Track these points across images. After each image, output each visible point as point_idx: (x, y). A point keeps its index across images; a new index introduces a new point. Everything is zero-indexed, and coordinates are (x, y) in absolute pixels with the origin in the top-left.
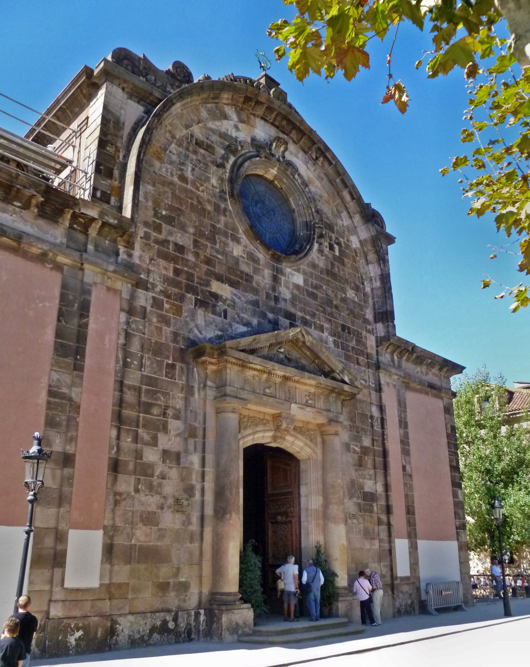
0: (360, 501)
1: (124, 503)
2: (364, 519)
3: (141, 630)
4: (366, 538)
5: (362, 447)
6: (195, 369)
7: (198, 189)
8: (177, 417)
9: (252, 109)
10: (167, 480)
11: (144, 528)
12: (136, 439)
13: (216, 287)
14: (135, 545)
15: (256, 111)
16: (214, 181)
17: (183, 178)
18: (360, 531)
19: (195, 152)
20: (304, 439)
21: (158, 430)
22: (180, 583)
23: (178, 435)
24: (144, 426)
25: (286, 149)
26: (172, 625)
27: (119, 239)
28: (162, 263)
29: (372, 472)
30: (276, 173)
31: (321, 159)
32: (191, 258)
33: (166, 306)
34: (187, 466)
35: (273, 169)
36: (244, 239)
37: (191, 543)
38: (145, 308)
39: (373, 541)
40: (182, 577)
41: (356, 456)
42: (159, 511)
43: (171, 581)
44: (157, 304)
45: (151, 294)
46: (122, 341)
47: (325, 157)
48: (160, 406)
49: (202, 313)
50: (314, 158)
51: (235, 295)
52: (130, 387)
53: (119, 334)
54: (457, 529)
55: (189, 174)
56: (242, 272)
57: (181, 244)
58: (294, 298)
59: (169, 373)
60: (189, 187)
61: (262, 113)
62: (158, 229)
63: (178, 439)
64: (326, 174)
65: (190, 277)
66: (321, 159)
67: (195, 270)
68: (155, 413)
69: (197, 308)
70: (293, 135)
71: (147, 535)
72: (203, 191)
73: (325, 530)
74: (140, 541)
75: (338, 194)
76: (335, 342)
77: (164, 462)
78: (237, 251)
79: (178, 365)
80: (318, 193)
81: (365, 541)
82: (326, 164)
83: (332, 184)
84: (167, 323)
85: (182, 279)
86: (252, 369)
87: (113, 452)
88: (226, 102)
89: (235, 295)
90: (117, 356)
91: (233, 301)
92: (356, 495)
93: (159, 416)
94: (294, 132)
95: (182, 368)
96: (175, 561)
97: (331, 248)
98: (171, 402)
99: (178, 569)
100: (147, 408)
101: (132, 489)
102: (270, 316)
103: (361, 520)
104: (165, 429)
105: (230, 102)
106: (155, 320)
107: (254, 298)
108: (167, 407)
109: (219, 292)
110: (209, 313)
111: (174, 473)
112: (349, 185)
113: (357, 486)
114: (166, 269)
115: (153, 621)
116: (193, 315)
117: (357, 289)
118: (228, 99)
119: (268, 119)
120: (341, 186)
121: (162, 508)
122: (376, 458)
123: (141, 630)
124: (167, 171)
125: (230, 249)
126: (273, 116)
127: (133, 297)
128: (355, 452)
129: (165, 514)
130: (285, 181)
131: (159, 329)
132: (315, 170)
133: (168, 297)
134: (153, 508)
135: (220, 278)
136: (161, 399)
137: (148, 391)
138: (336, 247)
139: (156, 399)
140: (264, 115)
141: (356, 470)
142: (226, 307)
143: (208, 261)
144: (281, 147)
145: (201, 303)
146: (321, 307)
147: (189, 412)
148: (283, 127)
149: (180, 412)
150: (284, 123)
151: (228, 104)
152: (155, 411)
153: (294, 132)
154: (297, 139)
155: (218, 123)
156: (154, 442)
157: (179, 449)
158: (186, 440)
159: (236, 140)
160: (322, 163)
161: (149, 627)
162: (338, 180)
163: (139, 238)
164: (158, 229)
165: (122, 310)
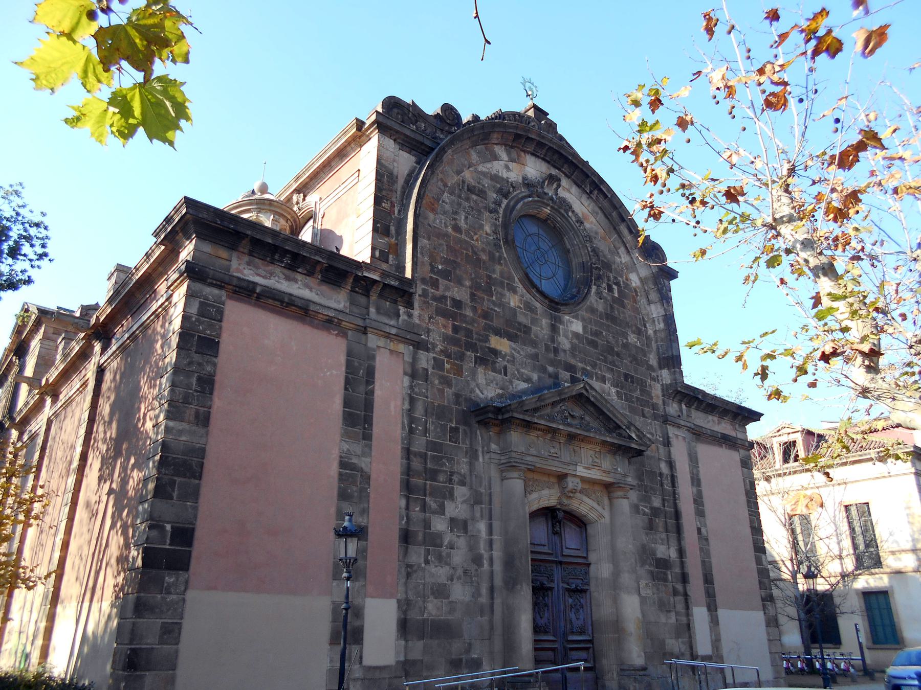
1: (415, 575)
5: (652, 508)
7: (472, 238)
8: (462, 483)
10: (456, 550)
11: (435, 601)
12: (424, 507)
13: (496, 342)
14: (428, 619)
16: (487, 228)
17: (457, 228)
19: (468, 199)
21: (444, 498)
22: (473, 659)
23: (464, 502)
24: (431, 495)
25: (559, 186)
27: (399, 299)
28: (441, 320)
29: (664, 536)
31: (596, 192)
32: (469, 313)
33: (447, 366)
34: (475, 534)
36: (520, 287)
38: (427, 370)
42: (449, 582)
43: (464, 657)
44: (438, 364)
45: (432, 355)
46: (407, 406)
47: (600, 190)
48: (446, 472)
51: (514, 349)
52: (416, 454)
53: (403, 399)
55: (462, 224)
56: (520, 324)
58: (574, 348)
60: (463, 236)
62: (435, 284)
63: (465, 506)
64: (600, 208)
65: (469, 333)
66: (596, 192)
67: (473, 326)
68: (441, 480)
71: (438, 609)
72: (477, 240)
73: (616, 600)
75: (615, 229)
77: (452, 531)
78: (513, 301)
79: (461, 428)
82: (601, 198)
83: (608, 219)
84: (449, 385)
87: (403, 522)
88: (496, 142)
89: (514, 349)
90: (403, 423)
91: (513, 356)
92: (649, 562)
94: (566, 166)
95: (464, 430)
97: (610, 289)
98: (456, 468)
99: (470, 644)
100: (432, 475)
101: (422, 560)
102: (550, 369)
104: (451, 497)
106: (437, 382)
107: (533, 351)
108: (452, 474)
109: (499, 348)
111: (462, 542)
114: (445, 327)
116: (474, 374)
117: (639, 332)
119: (539, 154)
121: (452, 580)
124: (441, 222)
125: (507, 300)
127: (415, 359)
128: (644, 514)
131: (441, 391)
133: (449, 356)
134: (443, 580)
135: (498, 333)
137: (433, 457)
138: (615, 287)
141: (647, 534)
142: (506, 363)
143: (486, 315)
145: (480, 361)
146: (602, 356)
147: (474, 478)
148: (555, 162)
149: (465, 478)
152: (441, 478)
155: (489, 165)
156: (441, 511)
158: (472, 506)
159: (507, 180)
162: (614, 214)
163: (417, 295)
164: (435, 284)
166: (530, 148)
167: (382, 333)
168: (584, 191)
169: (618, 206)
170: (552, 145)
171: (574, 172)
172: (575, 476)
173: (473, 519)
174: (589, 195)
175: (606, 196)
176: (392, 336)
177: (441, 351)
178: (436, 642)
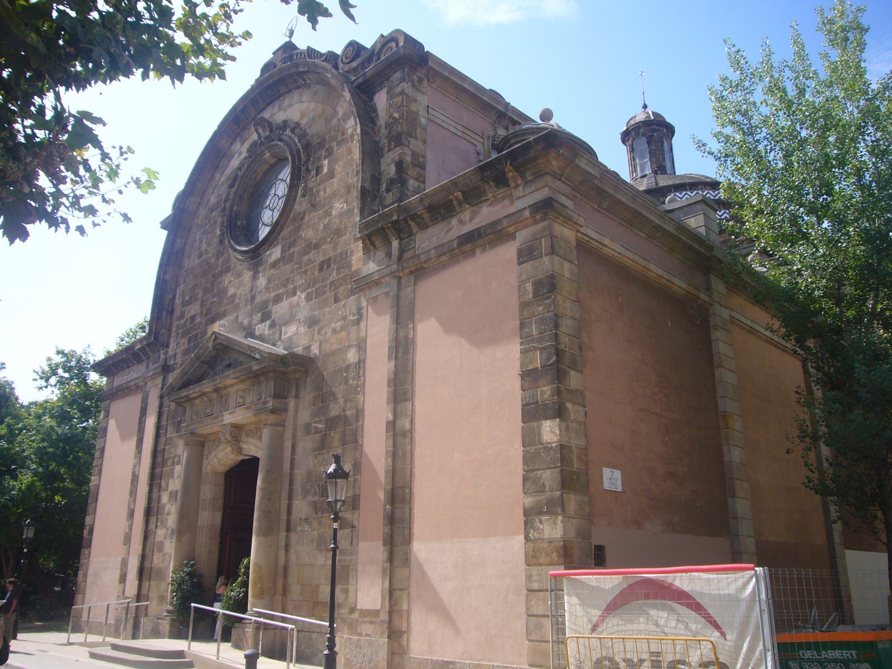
0: (316, 498)
2: (320, 523)
4: (320, 550)
18: (312, 541)
21: (169, 478)
30: (269, 154)
35: (265, 155)
41: (317, 437)
42: (164, 541)
54: (525, 515)
88: (228, 144)
92: (312, 491)
103: (315, 525)
119: (262, 107)
121: (166, 538)
134: (161, 539)
141: (316, 457)
160: (309, 78)
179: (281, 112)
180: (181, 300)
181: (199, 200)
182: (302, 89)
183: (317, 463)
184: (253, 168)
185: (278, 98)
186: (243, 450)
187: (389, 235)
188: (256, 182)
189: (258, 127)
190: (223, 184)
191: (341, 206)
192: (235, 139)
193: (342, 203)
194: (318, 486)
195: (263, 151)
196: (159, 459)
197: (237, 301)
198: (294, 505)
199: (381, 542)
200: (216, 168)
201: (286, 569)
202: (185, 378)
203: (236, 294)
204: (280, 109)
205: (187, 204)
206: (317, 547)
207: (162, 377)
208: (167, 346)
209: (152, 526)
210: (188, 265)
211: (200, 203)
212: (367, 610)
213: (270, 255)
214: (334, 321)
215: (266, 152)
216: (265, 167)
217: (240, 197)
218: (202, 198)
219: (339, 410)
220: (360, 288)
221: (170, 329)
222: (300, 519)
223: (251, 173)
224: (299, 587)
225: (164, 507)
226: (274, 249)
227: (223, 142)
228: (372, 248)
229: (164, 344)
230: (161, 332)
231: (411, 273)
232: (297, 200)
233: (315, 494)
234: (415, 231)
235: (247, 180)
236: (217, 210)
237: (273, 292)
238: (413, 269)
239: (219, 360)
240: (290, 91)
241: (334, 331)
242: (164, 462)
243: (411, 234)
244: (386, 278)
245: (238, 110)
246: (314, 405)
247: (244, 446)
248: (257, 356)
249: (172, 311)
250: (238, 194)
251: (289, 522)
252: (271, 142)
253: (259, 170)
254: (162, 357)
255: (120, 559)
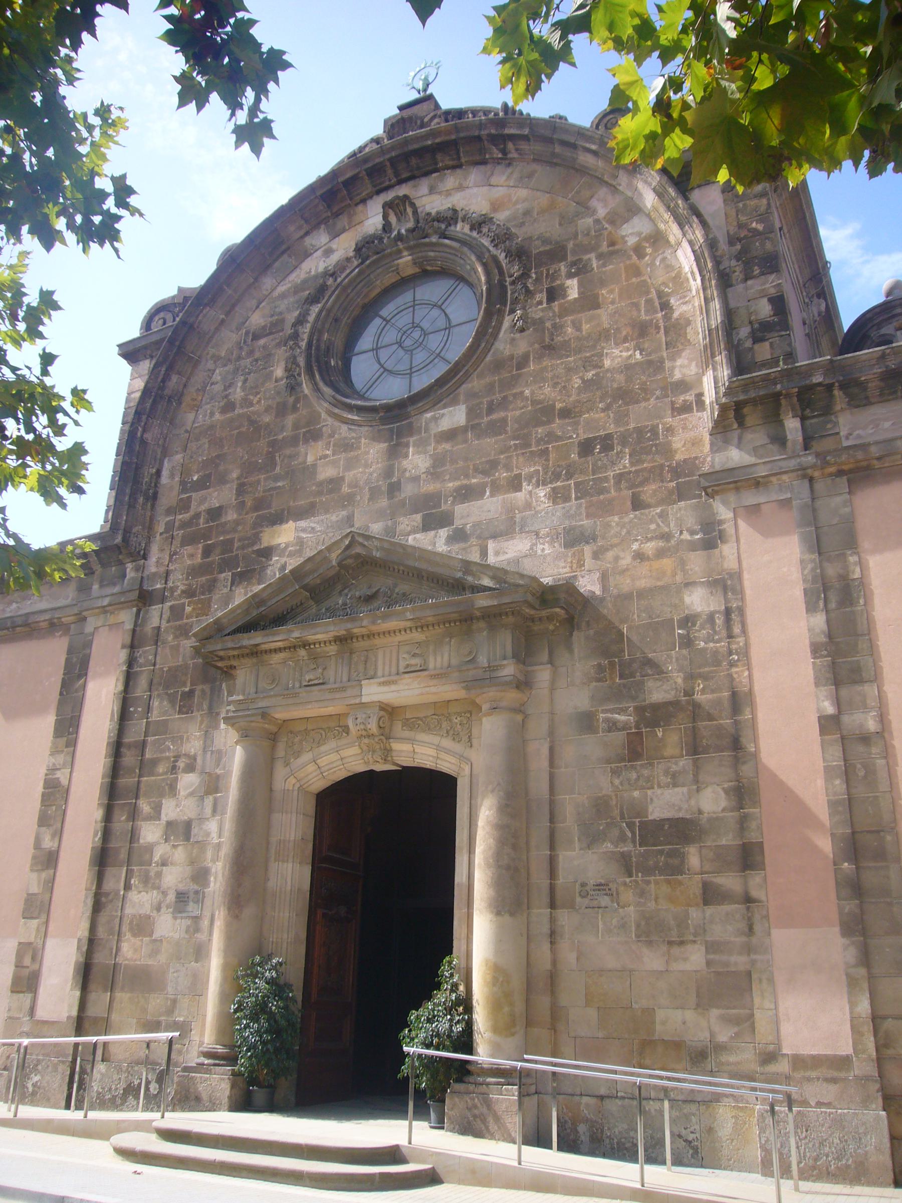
0: (627, 848)
2: (642, 894)
3: (113, 1087)
4: (650, 943)
5: (640, 710)
6: (224, 685)
8: (190, 768)
9: (351, 199)
15: (358, 194)
17: (229, 407)
18: (623, 926)
20: (436, 740)
21: (162, 795)
23: (191, 794)
26: (155, 1089)
27: (121, 557)
28: (189, 549)
29: (684, 763)
30: (410, 258)
31: (510, 146)
34: (200, 839)
35: (401, 258)
37: (196, 961)
38: (159, 628)
39: (676, 951)
40: (180, 1016)
41: (619, 738)
42: (154, 914)
44: (177, 613)
47: (512, 138)
48: (168, 758)
49: (242, 591)
50: (500, 156)
51: (304, 530)
52: (129, 746)
57: (217, 505)
59: (184, 706)
61: (369, 186)
64: (534, 160)
65: (227, 546)
66: (510, 146)
69: (233, 588)
70: (442, 161)
71: (136, 950)
72: (259, 402)
74: (127, 959)
76: (556, 496)
77: (166, 840)
80: (520, 211)
81: (645, 951)
82: (524, 146)
83: (556, 164)
85: (215, 557)
86: (271, 651)
87: (97, 839)
88: (302, 233)
89: (304, 530)
92: (615, 832)
93: (166, 773)
94: (439, 157)
95: (203, 691)
96: (170, 989)
99: (174, 1001)
103: (628, 896)
104: (172, 789)
105: (306, 228)
106: (170, 638)
108: (177, 757)
110: (254, 585)
111: (180, 855)
112: (572, 140)
113: (616, 813)
114: (191, 556)
115: (130, 1077)
118: (300, 228)
119: (387, 183)
120: (568, 153)
121: (158, 909)
122: (701, 724)
123: (113, 1087)
125: (301, 460)
126: (390, 171)
128: (613, 726)
129: (162, 918)
130: (432, 254)
132: (508, 178)
134: (146, 909)
136: (169, 749)
139: (163, 751)
140: (374, 186)
142: (283, 560)
143: (259, 504)
144: (405, 210)
149: (195, 760)
150: (414, 161)
151: (307, 234)
152: (161, 769)
153: (439, 157)
154: (453, 160)
156: (156, 813)
157: (190, 816)
160: (517, 150)
161: (123, 1085)
162: (558, 149)
163: (158, 537)
165: (123, 647)
166: (367, 187)
167: (97, 610)
168: (498, 161)
169: (548, 133)
170: (388, 156)
171: (458, 153)
172: (363, 705)
173: (201, 819)
174: (505, 160)
175: (525, 138)
176: (107, 608)
177: (183, 592)
178: (128, 995)
179: (435, 197)
180: (177, 479)
181: (222, 316)
182: (489, 166)
183: (621, 784)
184: (369, 275)
185: (427, 174)
186: (394, 754)
187: (783, 409)
188: (366, 301)
189: (391, 212)
190: (283, 296)
191: (625, 354)
192: (316, 227)
193: (628, 350)
194: (630, 826)
195: (399, 252)
196: (129, 759)
197: (345, 489)
198: (561, 858)
199: (837, 929)
200: (265, 268)
201: (553, 978)
202: (255, 613)
203: (342, 479)
204: (432, 190)
205: (200, 318)
206: (637, 936)
207: (135, 609)
208: (145, 557)
209: (109, 885)
210: (194, 422)
211: (223, 321)
212: (813, 1057)
213: (435, 419)
214: (637, 540)
215: (405, 253)
216: (390, 279)
217: (336, 320)
218: (228, 314)
219: (673, 693)
220: (716, 488)
221: (150, 528)
222: (583, 885)
223: (363, 283)
224: (592, 1013)
225: (150, 848)
226: (445, 411)
227: (292, 228)
228: (735, 426)
229: (139, 552)
230: (134, 530)
231: (840, 473)
232: (501, 334)
233: (622, 838)
234: (838, 407)
235: (352, 295)
236: (271, 337)
237: (450, 480)
238: (845, 467)
239: (339, 587)
240: (459, 166)
241: (640, 556)
242: (145, 767)
243: (827, 410)
244: (785, 477)
245: (341, 179)
246: (599, 680)
247: (396, 746)
248: (487, 582)
249: (155, 497)
250: (332, 315)
251: (552, 889)
252: (424, 238)
253: (378, 282)
254: (130, 573)
255: (10, 946)
